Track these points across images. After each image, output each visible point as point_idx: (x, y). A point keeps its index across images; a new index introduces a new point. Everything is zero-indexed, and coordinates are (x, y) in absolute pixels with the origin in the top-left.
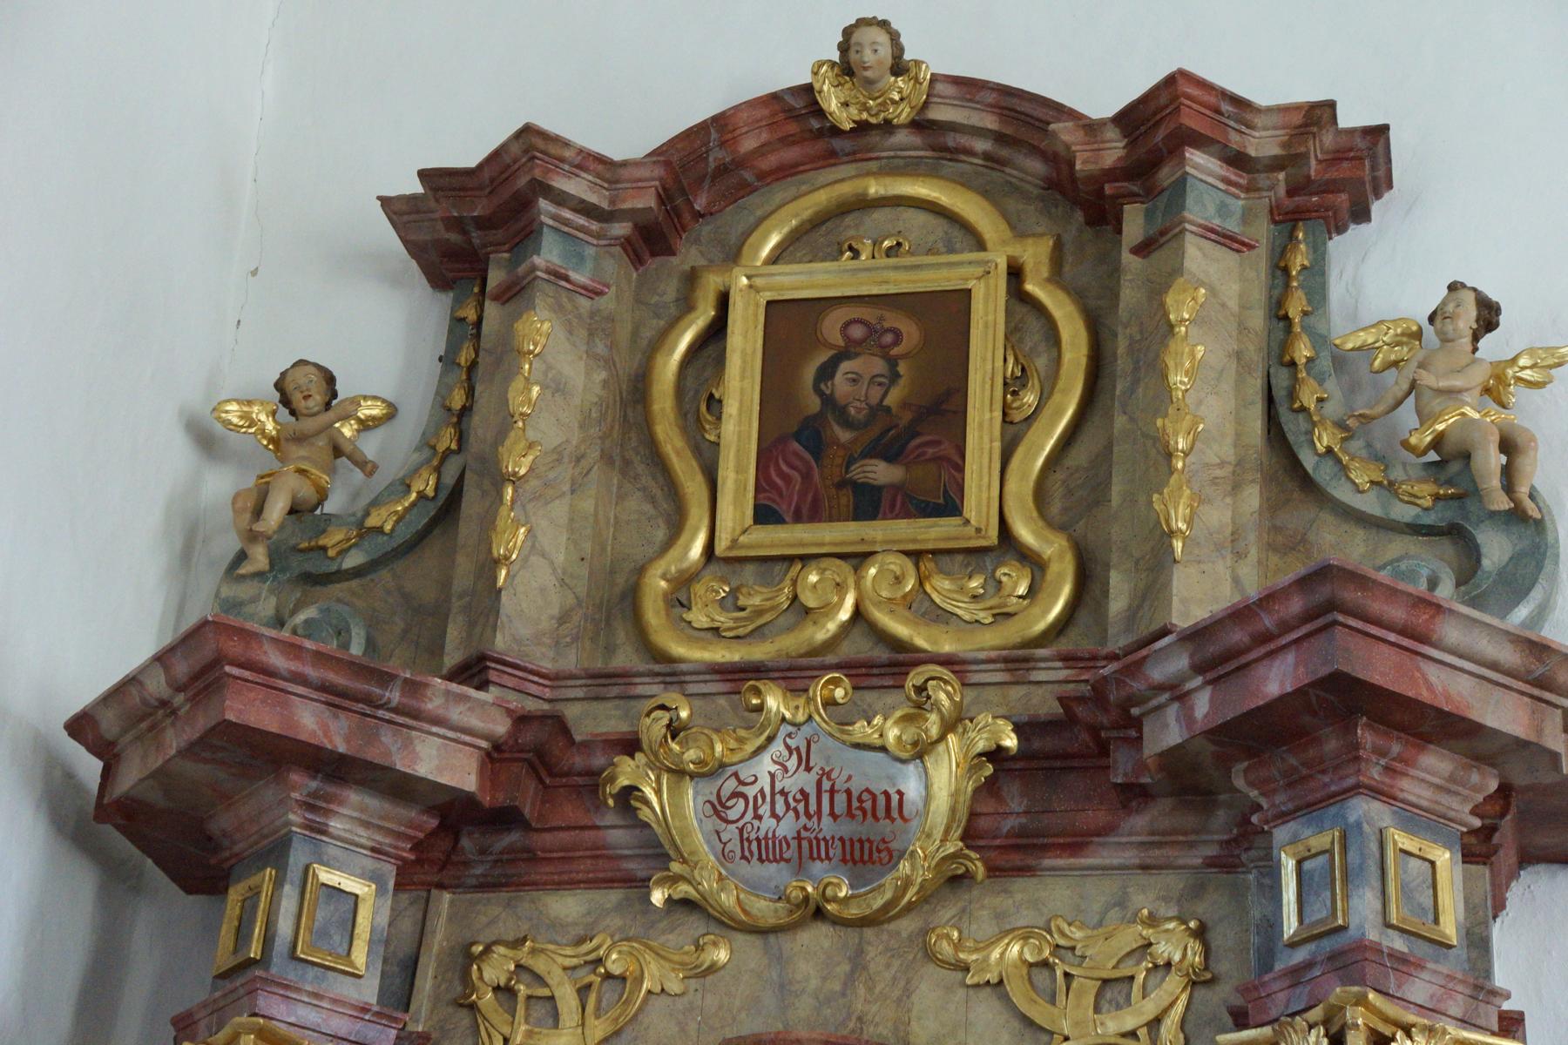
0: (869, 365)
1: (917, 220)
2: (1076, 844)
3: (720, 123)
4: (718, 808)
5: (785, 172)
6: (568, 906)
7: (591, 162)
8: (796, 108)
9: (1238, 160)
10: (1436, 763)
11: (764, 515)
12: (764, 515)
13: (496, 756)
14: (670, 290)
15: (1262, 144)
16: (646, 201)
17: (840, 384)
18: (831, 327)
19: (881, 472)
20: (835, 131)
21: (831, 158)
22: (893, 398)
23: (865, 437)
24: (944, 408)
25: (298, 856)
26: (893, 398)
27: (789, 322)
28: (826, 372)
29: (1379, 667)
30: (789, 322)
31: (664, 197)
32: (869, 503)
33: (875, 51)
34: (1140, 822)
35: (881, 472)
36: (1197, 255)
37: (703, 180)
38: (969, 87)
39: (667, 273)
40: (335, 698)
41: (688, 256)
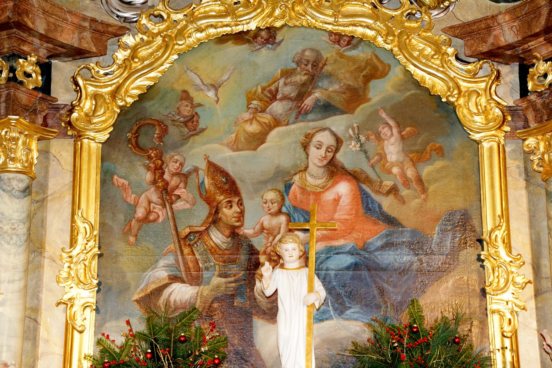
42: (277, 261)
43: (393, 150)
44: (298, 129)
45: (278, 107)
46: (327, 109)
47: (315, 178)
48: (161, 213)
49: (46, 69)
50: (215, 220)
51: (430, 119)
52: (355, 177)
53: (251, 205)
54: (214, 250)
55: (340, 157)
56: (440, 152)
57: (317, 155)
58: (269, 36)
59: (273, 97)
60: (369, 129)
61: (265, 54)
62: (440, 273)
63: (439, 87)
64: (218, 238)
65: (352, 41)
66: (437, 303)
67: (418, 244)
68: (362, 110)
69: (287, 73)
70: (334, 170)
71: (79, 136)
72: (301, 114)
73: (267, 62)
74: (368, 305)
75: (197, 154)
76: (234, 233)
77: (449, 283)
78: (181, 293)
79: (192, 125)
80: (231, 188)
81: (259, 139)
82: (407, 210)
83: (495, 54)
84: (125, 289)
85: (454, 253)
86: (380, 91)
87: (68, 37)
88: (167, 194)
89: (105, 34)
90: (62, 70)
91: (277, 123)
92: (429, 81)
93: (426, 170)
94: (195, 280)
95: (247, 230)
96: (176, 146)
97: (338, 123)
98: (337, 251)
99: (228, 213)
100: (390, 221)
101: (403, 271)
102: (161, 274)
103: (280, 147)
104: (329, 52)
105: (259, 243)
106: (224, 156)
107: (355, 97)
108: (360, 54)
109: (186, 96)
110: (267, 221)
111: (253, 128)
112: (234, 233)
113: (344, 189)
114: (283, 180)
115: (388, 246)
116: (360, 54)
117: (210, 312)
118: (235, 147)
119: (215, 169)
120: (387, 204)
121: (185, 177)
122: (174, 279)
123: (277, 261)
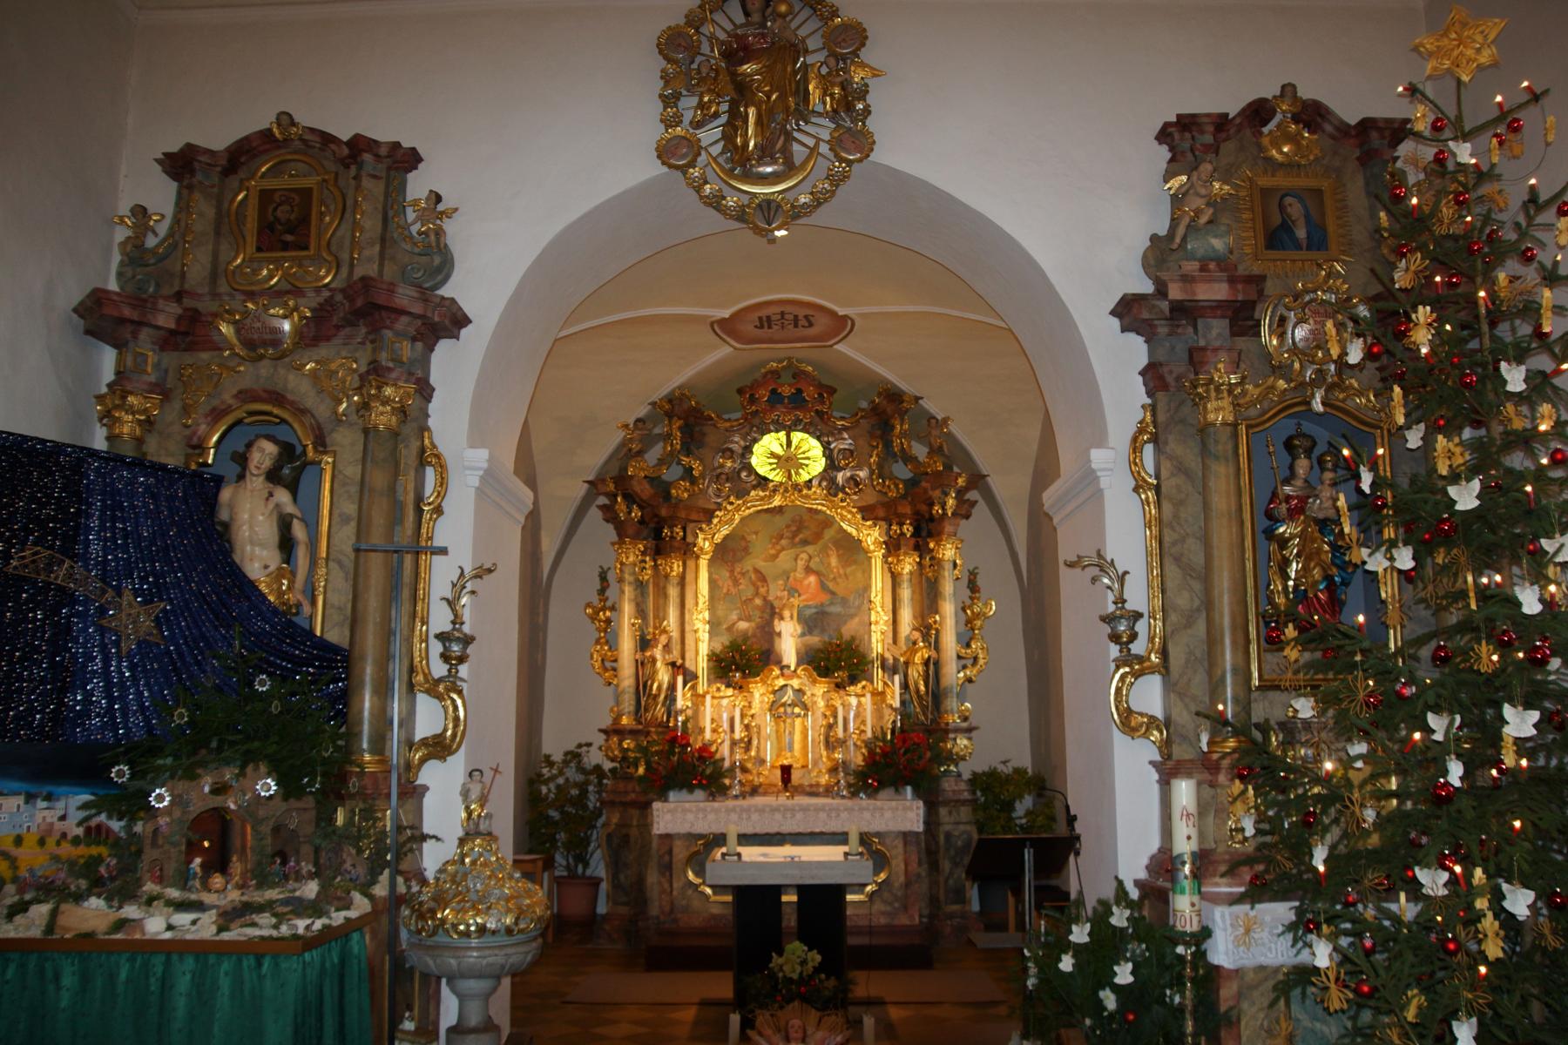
0: (286, 208)
1: (300, 165)
2: (328, 339)
3: (247, 139)
4: (238, 332)
5: (266, 151)
6: (205, 356)
7: (208, 151)
8: (266, 135)
9: (377, 156)
10: (404, 319)
11: (259, 249)
12: (259, 249)
13: (179, 319)
14: (236, 184)
15: (383, 151)
16: (224, 162)
17: (279, 213)
18: (277, 197)
19: (289, 238)
20: (277, 140)
21: (279, 147)
22: (293, 217)
23: (285, 228)
24: (305, 220)
25: (131, 345)
26: (293, 217)
27: (266, 196)
28: (275, 209)
29: (381, 300)
30: (266, 196)
31: (229, 161)
32: (286, 246)
33: (285, 119)
34: (343, 333)
35: (289, 238)
36: (367, 183)
37: (241, 155)
38: (312, 130)
39: (233, 181)
40: (134, 307)
41: (242, 174)
42: (782, 618)
43: (834, 561)
44: (792, 552)
45: (783, 542)
46: (805, 542)
47: (800, 574)
48: (733, 591)
49: (684, 529)
50: (757, 594)
51: (851, 548)
52: (817, 573)
53: (771, 587)
54: (757, 607)
55: (812, 564)
56: (855, 562)
57: (801, 563)
58: (780, 510)
59: (781, 537)
60: (824, 551)
61: (778, 518)
62: (852, 616)
63: (854, 533)
64: (758, 601)
65: (817, 512)
66: (849, 629)
67: (844, 601)
68: (821, 542)
69: (788, 526)
70: (808, 570)
71: (698, 557)
72: (793, 545)
73: (780, 522)
74: (823, 631)
75: (748, 564)
76: (765, 599)
77: (856, 620)
78: (743, 625)
79: (746, 550)
80: (763, 579)
81: (775, 557)
82: (840, 588)
83: (876, 519)
84: (719, 624)
85: (859, 607)
86: (829, 534)
87: (694, 516)
88: (736, 582)
89: (709, 515)
90: (690, 527)
91: (783, 549)
92: (849, 529)
93: (848, 570)
94: (748, 619)
95: (770, 598)
96: (740, 560)
97: (810, 549)
98: (809, 607)
99: (762, 590)
100: (833, 593)
101: (839, 615)
102: (734, 617)
103: (785, 558)
104: (806, 517)
105: (776, 604)
106: (761, 564)
107: (818, 536)
108: (820, 517)
109: (743, 538)
110: (779, 594)
111: (773, 552)
112: (765, 599)
113: (812, 579)
114: (786, 575)
115: (832, 604)
116: (820, 517)
117: (754, 635)
118: (765, 560)
119: (757, 571)
120: (831, 585)
121: (743, 574)
122: (740, 619)
123: (782, 618)
